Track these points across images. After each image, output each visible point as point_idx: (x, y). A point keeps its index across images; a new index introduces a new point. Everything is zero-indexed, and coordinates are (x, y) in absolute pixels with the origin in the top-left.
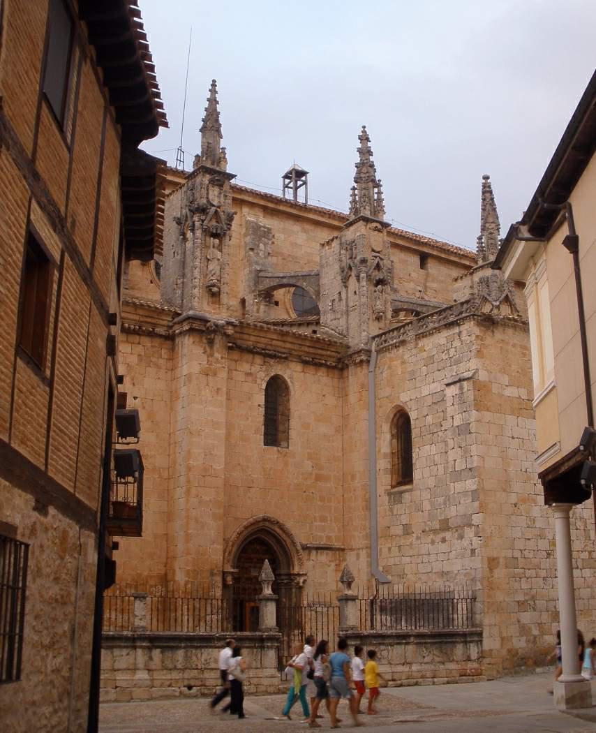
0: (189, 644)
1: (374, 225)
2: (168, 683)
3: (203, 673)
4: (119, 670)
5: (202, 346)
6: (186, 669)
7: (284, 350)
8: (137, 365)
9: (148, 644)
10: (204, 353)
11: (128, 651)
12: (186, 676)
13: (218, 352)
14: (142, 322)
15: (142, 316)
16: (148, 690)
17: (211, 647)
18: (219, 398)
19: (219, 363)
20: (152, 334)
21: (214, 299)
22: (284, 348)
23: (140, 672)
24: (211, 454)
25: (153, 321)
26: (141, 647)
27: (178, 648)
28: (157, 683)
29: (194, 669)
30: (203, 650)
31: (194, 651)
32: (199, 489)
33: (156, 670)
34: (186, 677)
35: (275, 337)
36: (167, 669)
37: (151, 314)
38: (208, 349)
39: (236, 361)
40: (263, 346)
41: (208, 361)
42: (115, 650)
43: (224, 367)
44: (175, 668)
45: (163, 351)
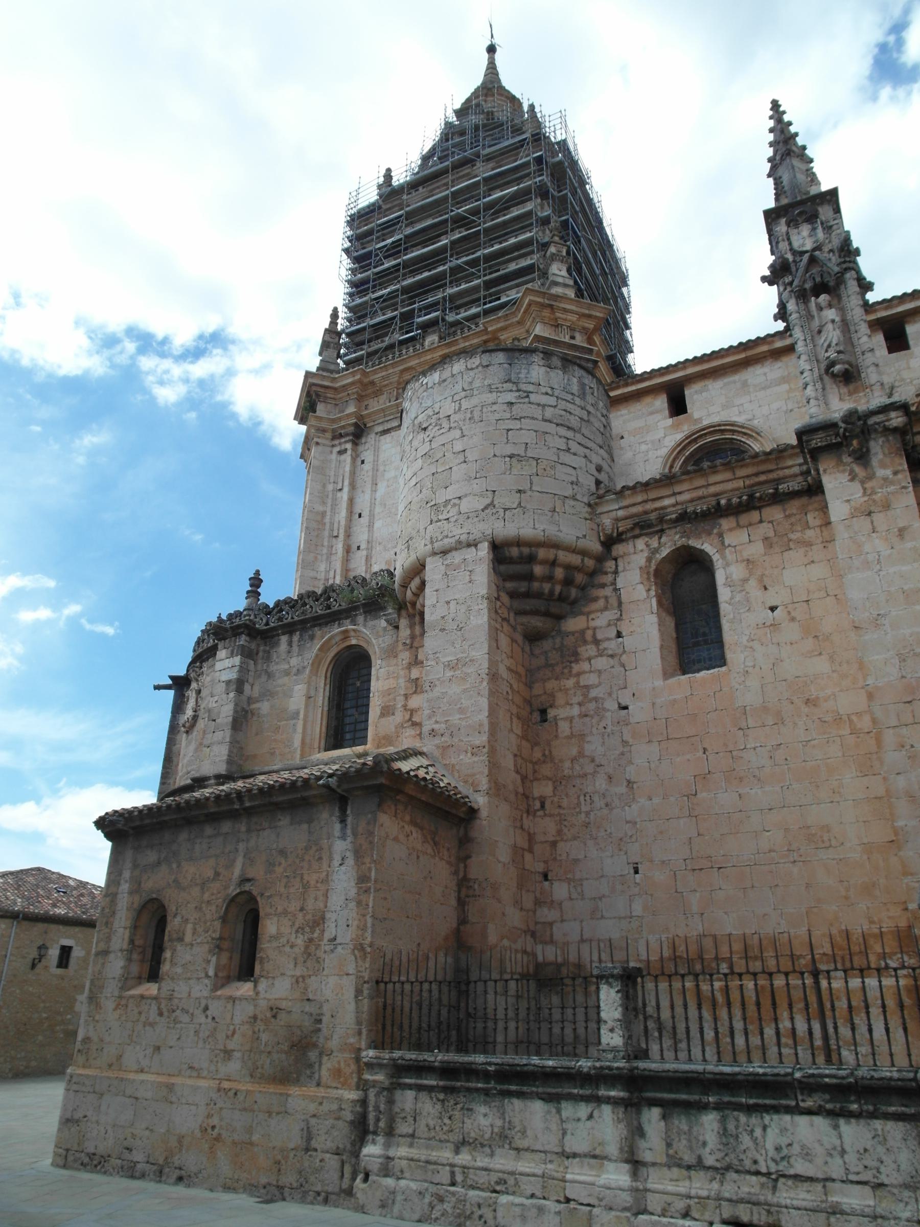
0: (726, 1099)
2: (680, 1205)
3: (775, 1188)
4: (575, 1155)
5: (844, 471)
6: (728, 1168)
8: (765, 554)
9: (622, 1094)
10: (852, 480)
11: (589, 1110)
12: (728, 1190)
13: (883, 466)
15: (748, 476)
16: (628, 1218)
17: (789, 1110)
19: (892, 483)
20: (778, 498)
21: (851, 387)
23: (610, 1166)
25: (771, 476)
26: (608, 1100)
27: (703, 1107)
28: (654, 1202)
29: (749, 1172)
30: (767, 1118)
31: (743, 1118)
32: (904, 731)
33: (654, 1164)
34: (727, 1195)
36: (679, 1166)
37: (763, 468)
38: (857, 469)
41: (865, 489)
42: (564, 1104)
44: (699, 1165)
45: (810, 517)
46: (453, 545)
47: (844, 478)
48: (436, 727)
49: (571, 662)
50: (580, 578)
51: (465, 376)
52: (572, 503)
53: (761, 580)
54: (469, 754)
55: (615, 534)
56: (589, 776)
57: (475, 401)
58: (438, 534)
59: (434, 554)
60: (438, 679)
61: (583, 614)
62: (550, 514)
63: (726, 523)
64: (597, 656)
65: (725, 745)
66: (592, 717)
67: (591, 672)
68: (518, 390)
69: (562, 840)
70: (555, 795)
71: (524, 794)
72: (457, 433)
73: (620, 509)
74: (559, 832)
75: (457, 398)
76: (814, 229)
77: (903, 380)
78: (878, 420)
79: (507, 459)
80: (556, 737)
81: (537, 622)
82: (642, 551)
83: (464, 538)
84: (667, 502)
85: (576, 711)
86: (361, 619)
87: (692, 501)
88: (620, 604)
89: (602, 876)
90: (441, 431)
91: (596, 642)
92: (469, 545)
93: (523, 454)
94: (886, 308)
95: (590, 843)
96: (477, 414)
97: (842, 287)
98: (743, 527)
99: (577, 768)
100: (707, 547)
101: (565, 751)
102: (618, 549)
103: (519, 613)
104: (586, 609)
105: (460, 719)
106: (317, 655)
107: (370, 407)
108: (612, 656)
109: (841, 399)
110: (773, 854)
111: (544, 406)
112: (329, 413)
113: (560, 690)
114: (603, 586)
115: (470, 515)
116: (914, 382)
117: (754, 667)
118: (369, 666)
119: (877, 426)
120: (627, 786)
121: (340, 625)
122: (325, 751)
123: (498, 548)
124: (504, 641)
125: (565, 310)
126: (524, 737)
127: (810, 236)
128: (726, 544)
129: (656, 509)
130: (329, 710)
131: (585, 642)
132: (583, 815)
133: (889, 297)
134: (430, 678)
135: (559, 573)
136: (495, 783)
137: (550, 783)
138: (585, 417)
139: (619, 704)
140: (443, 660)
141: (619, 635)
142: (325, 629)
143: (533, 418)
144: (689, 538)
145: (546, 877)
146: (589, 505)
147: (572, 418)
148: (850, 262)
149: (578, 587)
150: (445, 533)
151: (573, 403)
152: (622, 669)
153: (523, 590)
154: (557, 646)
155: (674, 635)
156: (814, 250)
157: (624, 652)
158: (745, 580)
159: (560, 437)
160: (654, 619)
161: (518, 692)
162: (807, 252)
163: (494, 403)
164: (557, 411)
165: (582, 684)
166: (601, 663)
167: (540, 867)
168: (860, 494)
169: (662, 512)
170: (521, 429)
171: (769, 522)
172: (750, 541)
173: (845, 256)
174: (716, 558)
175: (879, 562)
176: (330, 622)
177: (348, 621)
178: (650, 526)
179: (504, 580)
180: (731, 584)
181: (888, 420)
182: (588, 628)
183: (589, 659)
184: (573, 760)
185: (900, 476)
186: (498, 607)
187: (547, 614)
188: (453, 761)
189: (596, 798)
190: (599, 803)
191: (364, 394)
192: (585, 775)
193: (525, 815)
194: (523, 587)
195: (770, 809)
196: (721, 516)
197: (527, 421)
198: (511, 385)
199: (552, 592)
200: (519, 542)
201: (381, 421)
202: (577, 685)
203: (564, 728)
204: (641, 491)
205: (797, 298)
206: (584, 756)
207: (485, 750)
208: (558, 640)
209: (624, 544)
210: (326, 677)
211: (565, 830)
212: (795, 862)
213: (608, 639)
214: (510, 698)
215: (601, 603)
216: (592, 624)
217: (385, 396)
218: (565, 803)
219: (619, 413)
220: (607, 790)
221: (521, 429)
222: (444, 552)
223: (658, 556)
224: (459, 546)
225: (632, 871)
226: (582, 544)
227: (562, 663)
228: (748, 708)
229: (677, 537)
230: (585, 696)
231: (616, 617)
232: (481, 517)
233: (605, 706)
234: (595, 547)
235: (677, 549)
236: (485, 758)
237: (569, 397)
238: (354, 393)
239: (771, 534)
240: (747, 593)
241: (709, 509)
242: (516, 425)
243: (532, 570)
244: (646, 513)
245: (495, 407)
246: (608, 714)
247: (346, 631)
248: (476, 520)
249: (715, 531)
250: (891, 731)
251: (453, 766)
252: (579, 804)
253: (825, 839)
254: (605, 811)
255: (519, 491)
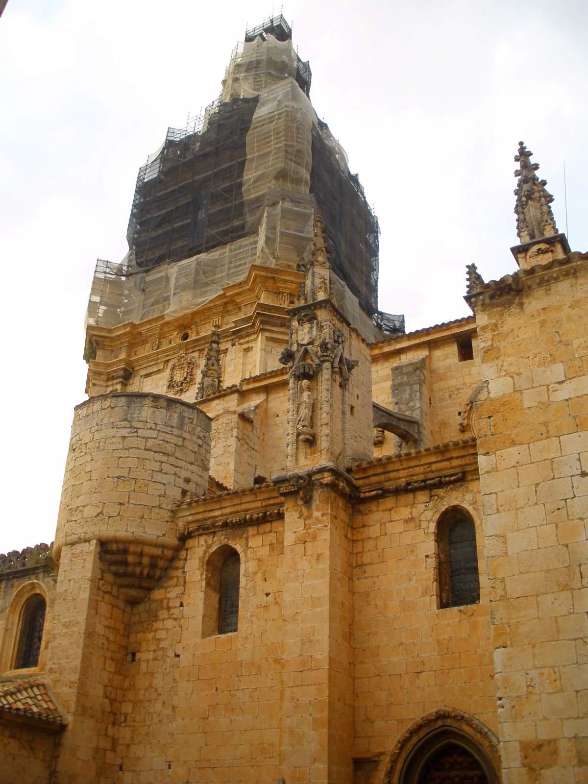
1: (535, 248)
5: (296, 511)
7: (452, 471)
8: (269, 556)
10: (300, 518)
13: (318, 510)
14: (266, 506)
15: (264, 499)
18: (321, 566)
19: (320, 522)
21: (313, 449)
22: (452, 468)
24: (311, 641)
32: (295, 689)
35: (433, 459)
38: (304, 510)
39: (390, 510)
40: (422, 477)
43: (326, 526)
46: (77, 540)
47: (296, 515)
48: (53, 666)
49: (153, 621)
50: (161, 563)
51: (99, 415)
52: (157, 510)
53: (264, 574)
54: (68, 687)
55: (186, 533)
56: (153, 701)
57: (102, 434)
58: (69, 531)
59: (67, 544)
60: (58, 634)
61: (162, 587)
62: (139, 520)
63: (251, 530)
64: (168, 619)
65: (228, 686)
66: (159, 661)
67: (163, 629)
68: (131, 427)
69: (133, 743)
70: (133, 713)
71: (111, 712)
72: (88, 457)
73: (190, 515)
74: (132, 738)
75: (93, 430)
76: (311, 328)
77: (464, 384)
78: (318, 478)
79: (116, 479)
80: (139, 672)
81: (134, 593)
82: (202, 545)
83: (82, 536)
84: (217, 513)
85: (151, 656)
86: (41, 576)
87: (231, 513)
88: (185, 582)
89: (151, 770)
90: (82, 454)
91: (169, 608)
92: (86, 541)
93: (127, 476)
94: (458, 327)
95: (148, 746)
96: (102, 444)
97: (320, 374)
98: (260, 534)
99: (147, 695)
100: (239, 548)
101: (141, 682)
102: (190, 543)
103: (121, 586)
104: (166, 585)
105: (66, 662)
106: (14, 599)
107: (138, 353)
108: (175, 619)
109: (306, 458)
110: (242, 760)
111: (147, 438)
112: (106, 358)
113: (145, 640)
114: (177, 569)
115: (88, 519)
116: (472, 386)
117: (251, 634)
118: (45, 609)
119: (316, 482)
120: (172, 710)
121: (29, 579)
122: (15, 669)
123: (104, 546)
124: (104, 608)
125: (285, 281)
126: (118, 672)
127: (309, 333)
128: (249, 546)
129: (210, 518)
130: (20, 639)
131: (162, 608)
132: (146, 727)
133: (459, 318)
134: (54, 632)
135: (146, 561)
136: (82, 706)
137: (131, 704)
138: (180, 444)
139: (175, 654)
140: (63, 621)
141: (182, 605)
142: (21, 581)
143: (138, 448)
144: (228, 540)
145: (121, 767)
146: (172, 511)
147: (168, 446)
148: (326, 356)
149: (161, 569)
150: (73, 532)
151: (172, 434)
152: (180, 629)
153: (121, 571)
154: (146, 609)
155: (217, 606)
156: (308, 344)
157: (183, 617)
158: (255, 573)
159: (156, 461)
160: (202, 595)
161: (115, 642)
162: (304, 345)
163: (114, 437)
164: (157, 442)
165: (157, 637)
166: (169, 623)
167: (119, 761)
168: (302, 528)
169: (214, 519)
170: (128, 457)
171: (275, 532)
172: (262, 546)
173: (324, 352)
174: (242, 555)
175: (303, 577)
176: (23, 576)
177: (34, 576)
178: (208, 528)
179: (110, 565)
180: (247, 575)
181: (323, 478)
182: (165, 598)
183: (163, 620)
184: (146, 689)
185: (325, 518)
186: (101, 584)
187: (140, 587)
188: (59, 691)
189: (155, 716)
190: (156, 720)
191: (134, 342)
192: (149, 701)
193: (110, 727)
194: (122, 569)
195: (245, 731)
196: (249, 525)
197: (134, 450)
198: (127, 422)
199: (141, 573)
200: (117, 541)
201: (145, 366)
202: (154, 638)
203: (143, 667)
204: (202, 504)
205: (295, 379)
206: (152, 687)
207: (76, 685)
208: (148, 605)
209: (193, 539)
210: (20, 615)
211: (135, 737)
212: (253, 766)
213: (175, 607)
214: (106, 646)
215: (175, 580)
216: (168, 595)
217: (149, 344)
218: (137, 719)
219: (278, 395)
220: (161, 711)
221: (128, 457)
222: (73, 544)
223: (210, 550)
224: (80, 541)
225: (167, 767)
226: (161, 540)
227: (149, 621)
228: (243, 662)
229: (223, 538)
230: (157, 645)
231: (181, 591)
232: (94, 522)
233: (167, 654)
234: (173, 541)
235: (223, 546)
236: (75, 690)
237: (168, 430)
238: (126, 342)
239: (274, 541)
240: (255, 582)
241: (240, 521)
242: (124, 454)
243: (127, 559)
244: (205, 519)
245: (114, 440)
246: (168, 660)
247: (33, 584)
248: (91, 523)
249: (245, 536)
250: (289, 689)
251: (59, 694)
252: (145, 720)
253: (271, 752)
254: (158, 725)
255: (120, 504)
